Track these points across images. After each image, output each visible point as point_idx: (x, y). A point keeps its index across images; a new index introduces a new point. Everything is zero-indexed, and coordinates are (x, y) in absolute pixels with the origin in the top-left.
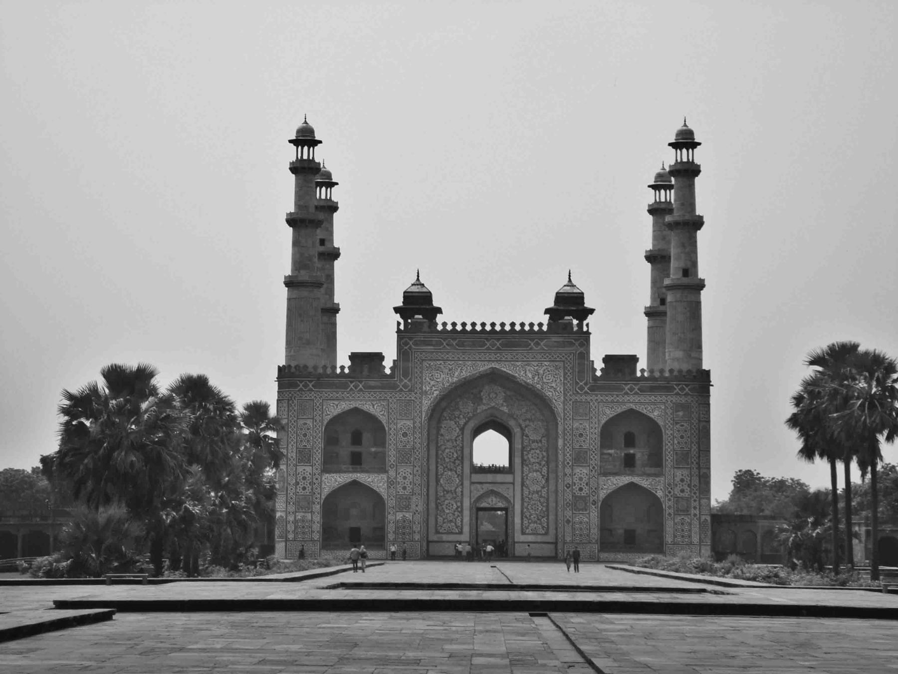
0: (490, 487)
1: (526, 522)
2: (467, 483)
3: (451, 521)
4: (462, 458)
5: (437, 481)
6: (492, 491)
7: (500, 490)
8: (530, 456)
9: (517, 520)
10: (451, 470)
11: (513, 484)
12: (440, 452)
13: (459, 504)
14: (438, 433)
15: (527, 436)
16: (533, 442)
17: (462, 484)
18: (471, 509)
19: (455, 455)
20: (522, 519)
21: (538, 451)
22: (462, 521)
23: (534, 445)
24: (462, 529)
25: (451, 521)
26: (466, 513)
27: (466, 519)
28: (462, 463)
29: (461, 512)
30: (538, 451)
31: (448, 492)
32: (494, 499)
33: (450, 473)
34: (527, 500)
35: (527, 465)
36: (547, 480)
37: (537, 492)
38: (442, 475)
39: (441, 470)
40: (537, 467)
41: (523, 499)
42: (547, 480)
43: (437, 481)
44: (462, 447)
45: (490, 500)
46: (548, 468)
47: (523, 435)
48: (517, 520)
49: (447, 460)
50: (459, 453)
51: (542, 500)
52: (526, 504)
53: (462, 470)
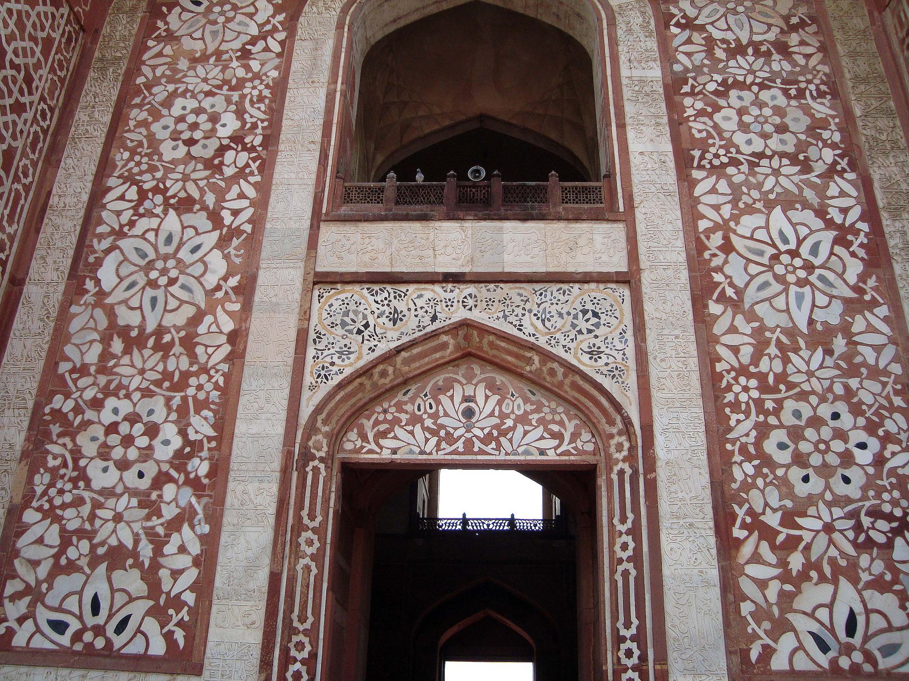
0: (455, 306)
1: (759, 571)
2: (280, 280)
3: (117, 557)
4: (271, 139)
5: (82, 268)
6: (465, 324)
7: (530, 329)
8: (727, 119)
9: (687, 554)
10: (185, 205)
11: (629, 279)
12: (137, 115)
13: (201, 426)
14: (148, 29)
15: (688, 24)
16: (738, 50)
17: (246, 290)
18: (295, 461)
19: (229, 124)
20: (727, 546)
21: (774, 96)
22: (207, 561)
23: (738, 68)
24: (198, 625)
25: (117, 557)
26: (253, 494)
27: (247, 542)
28: (266, 167)
29: (213, 487)
30: (774, 96)
31: (134, 341)
32: (486, 405)
33: (172, 222)
34: (744, 391)
35: (718, 170)
36: (877, 257)
37: (820, 338)
38: (120, 234)
39: (118, 203)
40: (790, 178)
41: (713, 385)
42: (877, 257)
43: (82, 268)
44: (280, 89)
45: (451, 407)
46: (866, 184)
47: (664, 21)
48: (687, 554)
49: (170, 151)
50: (256, 113)
51: (868, 392)
52: (743, 428)
53: (261, 204)
